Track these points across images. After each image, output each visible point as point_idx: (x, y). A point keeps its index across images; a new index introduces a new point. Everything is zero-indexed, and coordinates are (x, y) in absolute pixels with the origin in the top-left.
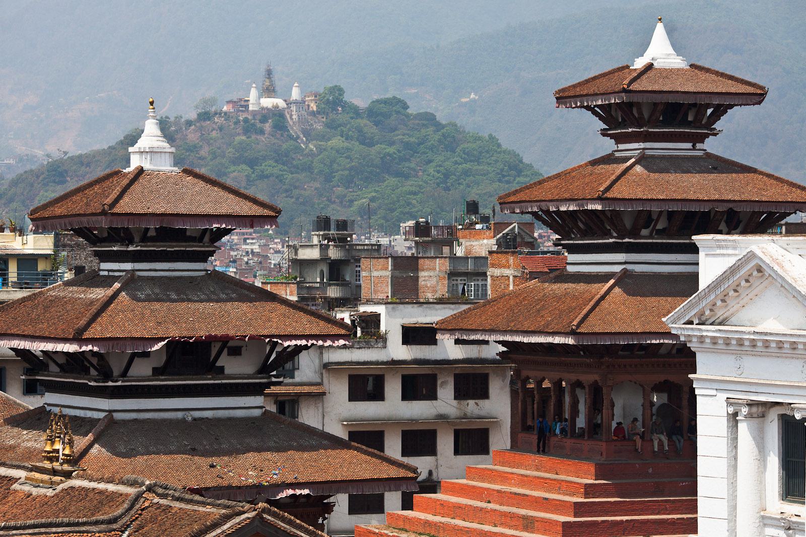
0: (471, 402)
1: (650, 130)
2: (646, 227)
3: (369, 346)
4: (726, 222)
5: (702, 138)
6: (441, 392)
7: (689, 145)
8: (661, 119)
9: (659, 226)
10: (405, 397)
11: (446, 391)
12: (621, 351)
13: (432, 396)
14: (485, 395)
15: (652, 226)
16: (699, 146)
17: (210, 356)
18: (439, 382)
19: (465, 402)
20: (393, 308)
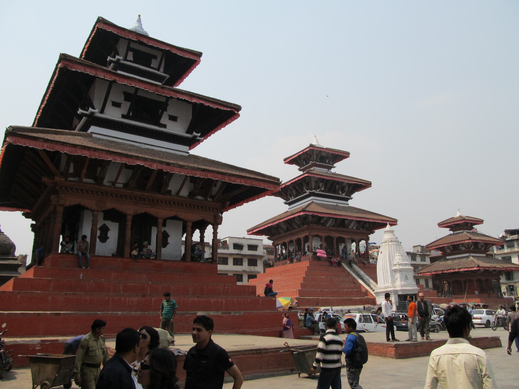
0: (253, 267)
1: (317, 163)
2: (318, 189)
3: (224, 249)
4: (341, 191)
5: (330, 168)
6: (244, 263)
7: (327, 170)
9: (322, 189)
10: (234, 264)
11: (245, 263)
12: (315, 224)
13: (242, 264)
14: (256, 265)
15: (320, 189)
16: (329, 170)
17: (165, 59)
18: (243, 261)
19: (251, 267)
20: (231, 239)
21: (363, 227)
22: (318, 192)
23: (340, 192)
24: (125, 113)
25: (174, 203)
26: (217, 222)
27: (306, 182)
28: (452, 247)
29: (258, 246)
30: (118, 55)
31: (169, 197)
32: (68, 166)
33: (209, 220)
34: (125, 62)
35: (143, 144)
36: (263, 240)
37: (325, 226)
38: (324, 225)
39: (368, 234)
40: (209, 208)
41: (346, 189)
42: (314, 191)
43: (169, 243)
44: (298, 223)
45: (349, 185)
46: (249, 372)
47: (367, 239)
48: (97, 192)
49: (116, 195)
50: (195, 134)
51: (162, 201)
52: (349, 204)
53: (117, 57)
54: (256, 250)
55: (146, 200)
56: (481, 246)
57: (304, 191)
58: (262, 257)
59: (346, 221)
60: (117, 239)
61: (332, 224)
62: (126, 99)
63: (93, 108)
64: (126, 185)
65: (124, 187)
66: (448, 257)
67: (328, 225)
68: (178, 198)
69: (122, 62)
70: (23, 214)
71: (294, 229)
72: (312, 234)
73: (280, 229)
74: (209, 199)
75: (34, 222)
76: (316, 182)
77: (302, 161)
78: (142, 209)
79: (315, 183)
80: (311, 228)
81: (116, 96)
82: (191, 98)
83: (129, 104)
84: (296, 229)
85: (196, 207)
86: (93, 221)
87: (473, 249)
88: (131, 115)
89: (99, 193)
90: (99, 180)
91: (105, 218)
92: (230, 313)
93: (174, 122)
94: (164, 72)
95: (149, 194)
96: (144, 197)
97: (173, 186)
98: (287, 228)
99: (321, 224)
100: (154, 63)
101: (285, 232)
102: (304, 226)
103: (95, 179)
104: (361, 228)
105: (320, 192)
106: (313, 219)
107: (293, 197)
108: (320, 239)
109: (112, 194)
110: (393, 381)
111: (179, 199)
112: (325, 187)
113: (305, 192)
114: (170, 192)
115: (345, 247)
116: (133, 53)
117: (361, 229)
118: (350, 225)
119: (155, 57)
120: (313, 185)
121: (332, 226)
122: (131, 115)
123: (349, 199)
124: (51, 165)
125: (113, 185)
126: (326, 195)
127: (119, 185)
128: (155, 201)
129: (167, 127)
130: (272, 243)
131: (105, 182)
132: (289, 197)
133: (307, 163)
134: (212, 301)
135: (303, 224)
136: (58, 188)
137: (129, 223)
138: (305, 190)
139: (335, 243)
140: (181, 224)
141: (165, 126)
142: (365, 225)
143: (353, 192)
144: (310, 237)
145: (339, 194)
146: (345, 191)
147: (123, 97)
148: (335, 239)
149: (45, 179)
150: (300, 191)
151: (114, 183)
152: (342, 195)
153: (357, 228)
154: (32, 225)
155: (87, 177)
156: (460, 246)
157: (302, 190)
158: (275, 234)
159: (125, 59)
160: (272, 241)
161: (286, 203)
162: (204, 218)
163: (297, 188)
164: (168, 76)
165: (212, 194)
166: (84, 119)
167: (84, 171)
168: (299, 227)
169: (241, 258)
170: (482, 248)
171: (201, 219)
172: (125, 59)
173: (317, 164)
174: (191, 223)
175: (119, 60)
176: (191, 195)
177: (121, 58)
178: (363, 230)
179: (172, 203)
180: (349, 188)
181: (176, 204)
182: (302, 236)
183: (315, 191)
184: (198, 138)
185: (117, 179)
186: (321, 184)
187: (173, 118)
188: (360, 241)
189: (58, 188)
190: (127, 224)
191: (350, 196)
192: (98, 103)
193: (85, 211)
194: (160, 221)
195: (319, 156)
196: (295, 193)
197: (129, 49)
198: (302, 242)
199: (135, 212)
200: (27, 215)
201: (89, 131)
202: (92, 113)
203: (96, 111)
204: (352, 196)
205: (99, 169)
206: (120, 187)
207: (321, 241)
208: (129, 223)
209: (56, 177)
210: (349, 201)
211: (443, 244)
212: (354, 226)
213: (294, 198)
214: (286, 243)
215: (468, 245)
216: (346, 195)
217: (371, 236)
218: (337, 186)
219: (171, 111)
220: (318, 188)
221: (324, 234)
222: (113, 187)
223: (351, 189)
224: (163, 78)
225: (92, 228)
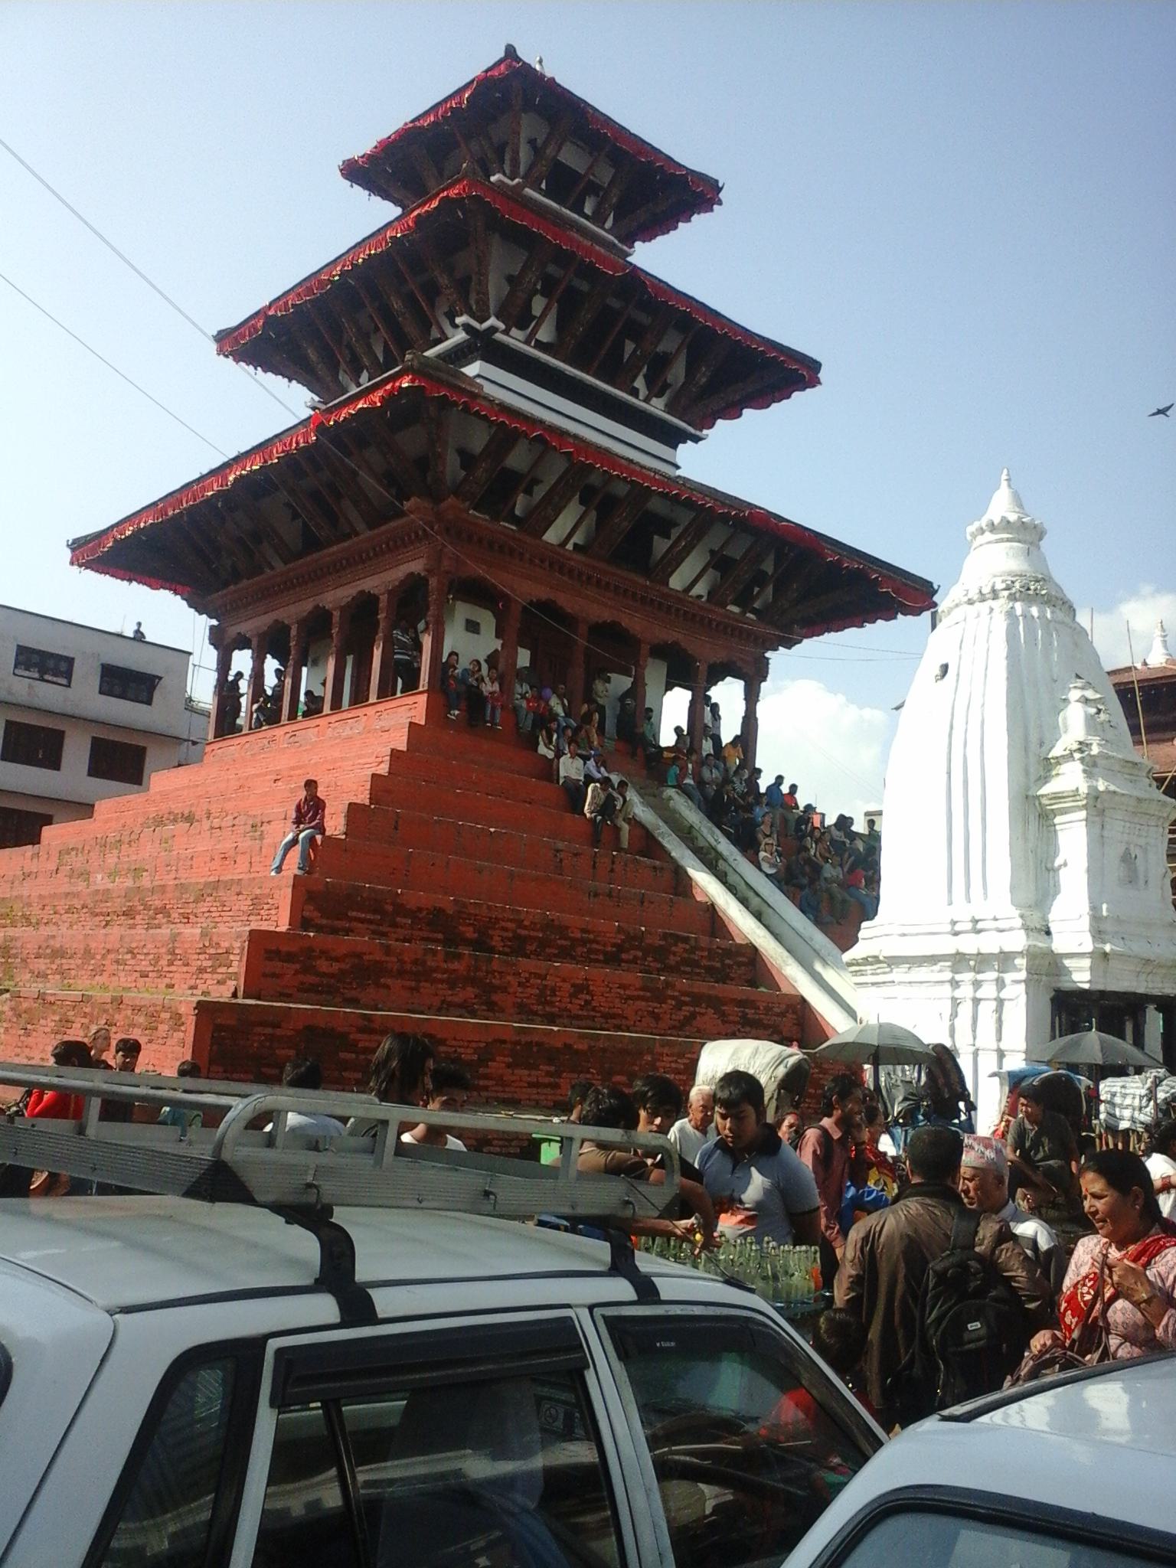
2: (522, 328)
4: (645, 376)
8: (543, 186)
12: (475, 509)
13: (53, 762)
21: (744, 600)
29: (160, 678)
36: (190, 654)
39: (763, 642)
41: (677, 373)
42: (492, 321)
47: (754, 677)
52: (678, 467)
54: (149, 702)
57: (435, 334)
67: (552, 536)
79: (507, 289)
104: (735, 603)
105: (527, 342)
106: (463, 473)
112: (561, 327)
117: (735, 609)
121: (575, 545)
130: (212, 628)
132: (343, 377)
142: (756, 589)
144: (433, 582)
145: (635, 393)
146: (666, 386)
150: (411, 330)
160: (211, 618)
173: (531, 199)
178: (744, 613)
182: (379, 582)
183: (502, 326)
186: (538, 305)
188: (715, 678)
210: (681, 446)
214: (288, 628)
218: (629, 347)
221: (525, 588)
223: (704, 380)
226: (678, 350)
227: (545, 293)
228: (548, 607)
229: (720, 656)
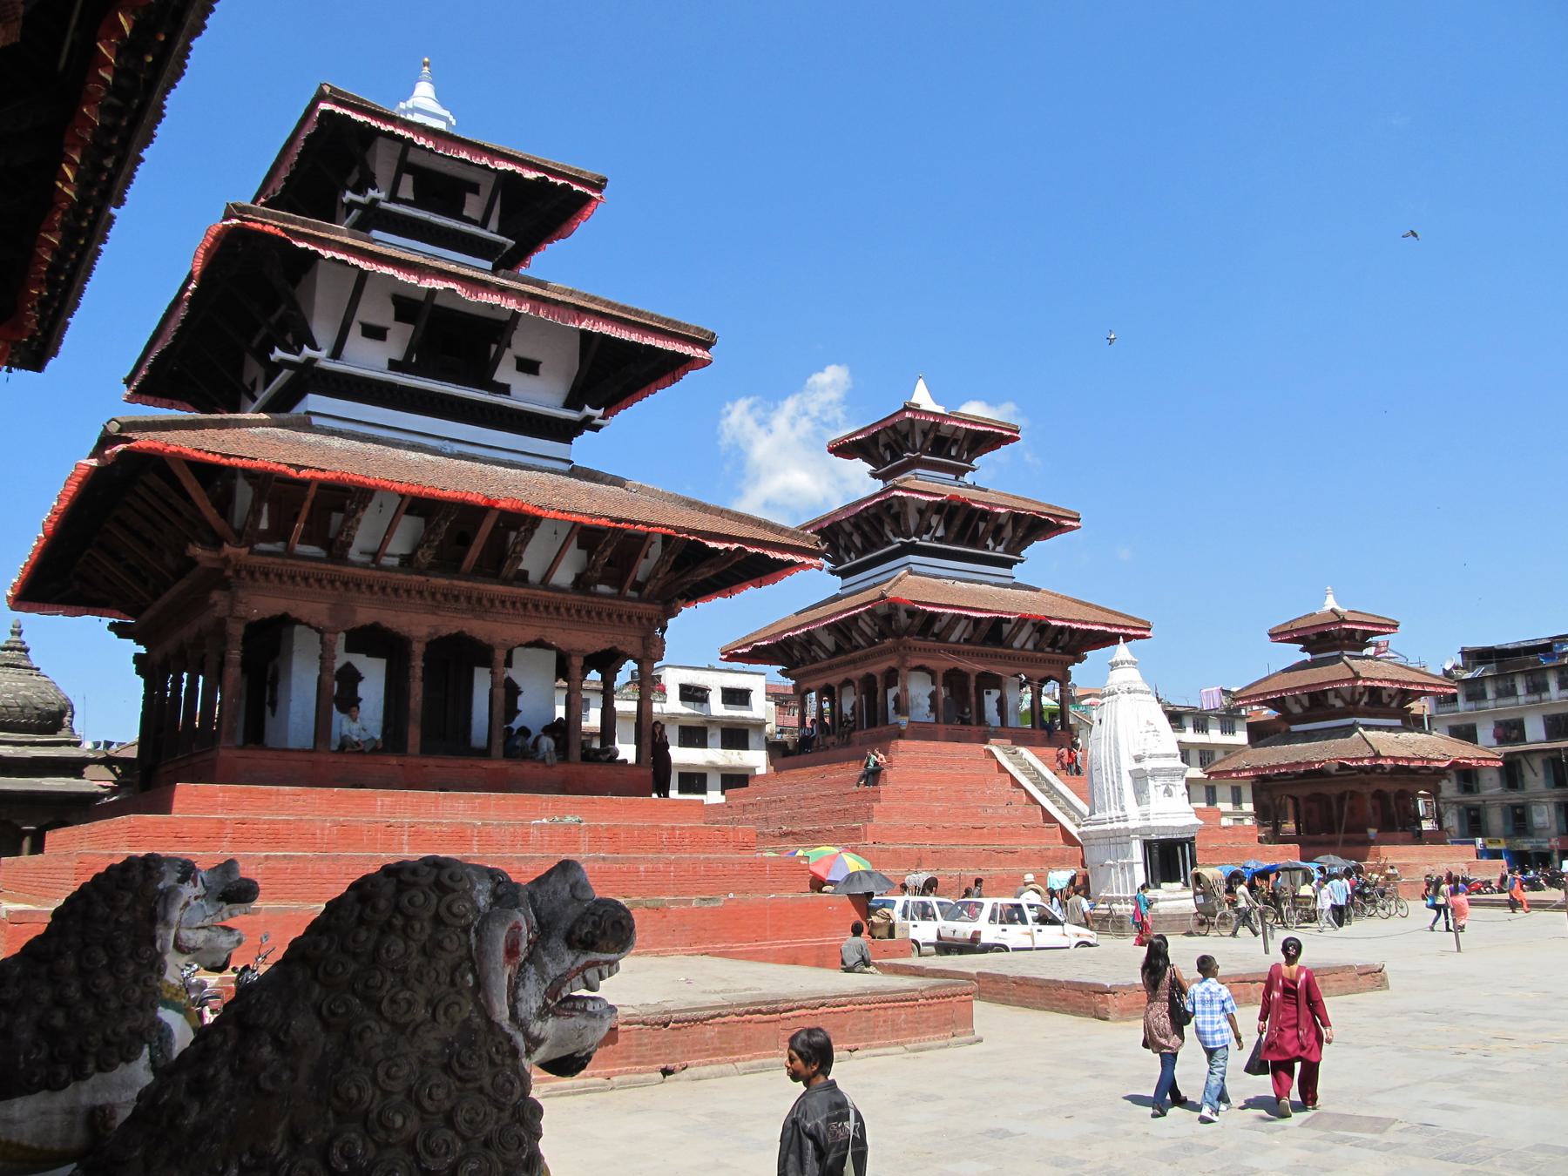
2: (927, 534)
7: (953, 477)
16: (961, 478)
18: (709, 734)
21: (1053, 644)
22: (925, 541)
23: (990, 542)
24: (398, 355)
25: (536, 607)
26: (650, 653)
27: (892, 511)
28: (1306, 697)
30: (373, 189)
31: (522, 591)
32: (256, 512)
33: (629, 650)
34: (393, 207)
35: (447, 442)
37: (945, 640)
38: (941, 637)
40: (630, 617)
41: (1008, 532)
43: (519, 711)
44: (868, 630)
45: (1016, 518)
46: (750, 1056)
47: (1064, 679)
48: (332, 582)
49: (383, 589)
50: (588, 410)
51: (503, 602)
53: (372, 193)
55: (462, 599)
56: (1390, 696)
57: (886, 539)
58: (760, 725)
59: (1004, 625)
60: (382, 703)
61: (965, 636)
62: (400, 317)
63: (314, 347)
64: (407, 561)
65: (401, 564)
66: (1294, 728)
67: (953, 638)
68: (544, 593)
69: (384, 205)
70: (112, 627)
71: (857, 648)
72: (908, 664)
73: (814, 647)
74: (630, 593)
75: (142, 650)
76: (921, 512)
77: (881, 449)
78: (451, 623)
79: (918, 516)
80: (905, 648)
81: (376, 310)
82: (578, 316)
83: (408, 330)
84: (864, 648)
85: (594, 614)
86: (321, 657)
87: (1366, 703)
88: (414, 359)
89: (338, 584)
90: (336, 550)
91: (350, 648)
92: (690, 902)
93: (532, 377)
94: (499, 233)
95: (469, 584)
96: (456, 593)
97: (533, 559)
98: (836, 643)
99: (934, 635)
100: (473, 206)
101: (830, 658)
102: (887, 641)
103: (327, 544)
105: (931, 541)
106: (910, 621)
107: (853, 555)
108: (930, 678)
109: (370, 587)
110: (1090, 1076)
111: (550, 594)
112: (946, 528)
113: (890, 543)
114: (522, 577)
115: (1001, 703)
116: (414, 179)
117: (1049, 649)
118: (1015, 637)
119: (474, 188)
120: (913, 521)
122: (414, 359)
123: (1015, 562)
124: (211, 514)
125: (373, 562)
126: (949, 550)
127: (390, 559)
128: (485, 602)
129: (512, 391)
131: (353, 554)
132: (841, 553)
133: (895, 457)
134: (642, 869)
135: (882, 635)
136: (229, 573)
137: (418, 665)
138: (887, 537)
139: (972, 690)
140: (552, 655)
141: (504, 389)
143: (1025, 541)
145: (987, 547)
146: (1003, 539)
147: (391, 310)
148: (973, 678)
149: (196, 551)
150: (875, 538)
151: (376, 555)
152: (994, 550)
153: (1036, 648)
154: (138, 658)
155: (306, 539)
156: (1331, 695)
157: (881, 535)
158: (803, 661)
159: (393, 198)
161: (833, 572)
162: (615, 644)
163: (866, 528)
164: (510, 241)
165: (638, 579)
166: (285, 374)
167: (300, 526)
168: (872, 643)
169: (701, 725)
170: (1391, 702)
171: (607, 646)
172: (393, 198)
174: (582, 659)
175: (375, 201)
176: (582, 583)
177: (382, 195)
179: (530, 606)
180: (1014, 530)
181: (542, 608)
182: (878, 668)
184: (597, 421)
185: (384, 543)
186: (934, 520)
187: (528, 366)
188: (1044, 681)
189: (229, 573)
190: (413, 664)
191: (1019, 555)
192: (323, 332)
193: (298, 628)
194: (500, 655)
195: (931, 436)
196: (859, 545)
197: (404, 167)
198: (879, 685)
199: (433, 631)
200: (121, 631)
201: (299, 409)
202: (312, 361)
203: (321, 354)
204: (1023, 553)
205: (337, 518)
206: (392, 566)
207: (933, 683)
208: (418, 665)
209: (226, 546)
211: (1281, 691)
212: (1029, 637)
213: (857, 558)
214: (833, 688)
215: (1353, 693)
216: (1006, 551)
217: (1075, 669)
218: (982, 526)
219: (521, 345)
220: (928, 529)
222: (374, 565)
224: (498, 246)
225: (320, 678)
226: (1008, 522)
227: (937, 513)
228: (955, 669)
229: (1042, 673)
